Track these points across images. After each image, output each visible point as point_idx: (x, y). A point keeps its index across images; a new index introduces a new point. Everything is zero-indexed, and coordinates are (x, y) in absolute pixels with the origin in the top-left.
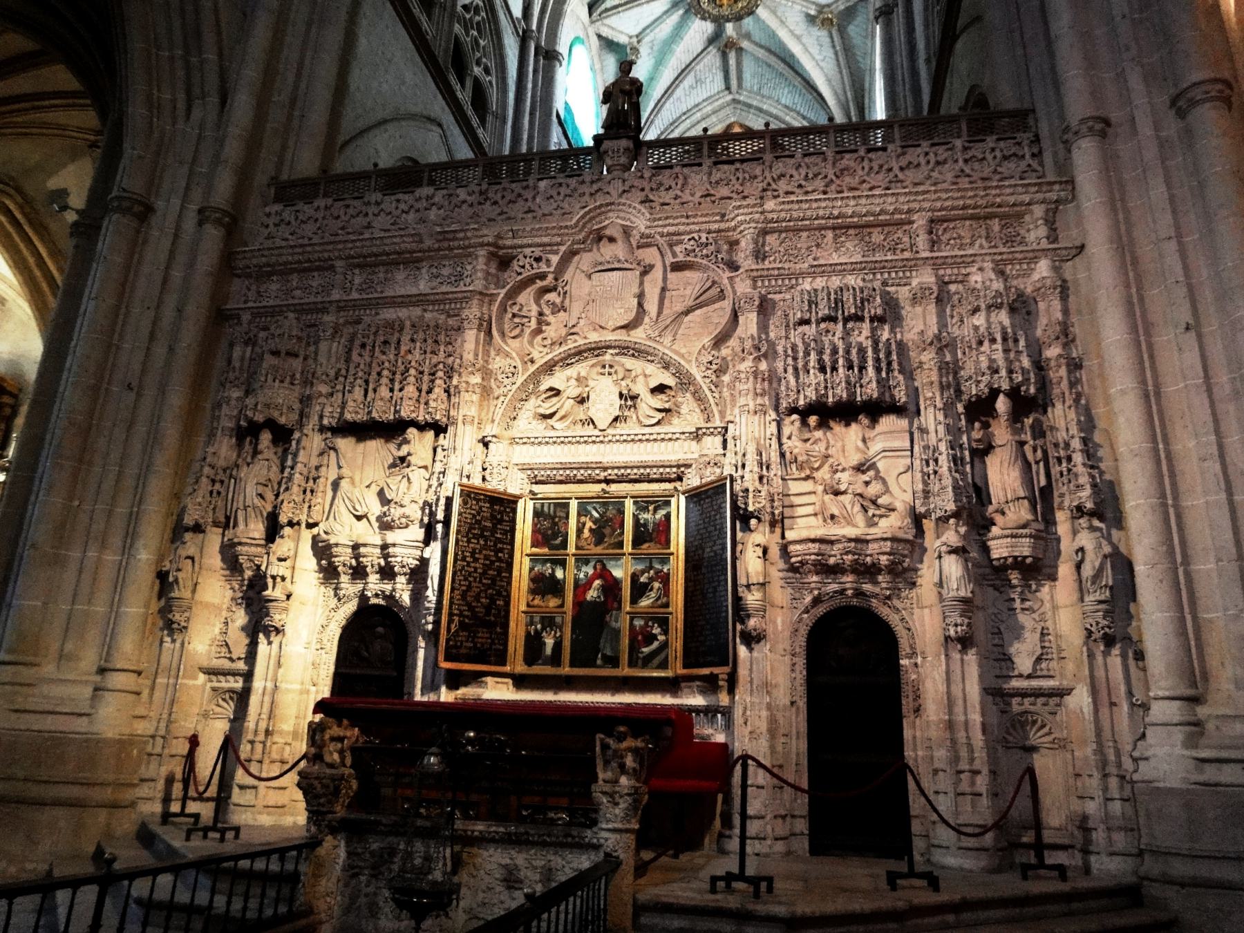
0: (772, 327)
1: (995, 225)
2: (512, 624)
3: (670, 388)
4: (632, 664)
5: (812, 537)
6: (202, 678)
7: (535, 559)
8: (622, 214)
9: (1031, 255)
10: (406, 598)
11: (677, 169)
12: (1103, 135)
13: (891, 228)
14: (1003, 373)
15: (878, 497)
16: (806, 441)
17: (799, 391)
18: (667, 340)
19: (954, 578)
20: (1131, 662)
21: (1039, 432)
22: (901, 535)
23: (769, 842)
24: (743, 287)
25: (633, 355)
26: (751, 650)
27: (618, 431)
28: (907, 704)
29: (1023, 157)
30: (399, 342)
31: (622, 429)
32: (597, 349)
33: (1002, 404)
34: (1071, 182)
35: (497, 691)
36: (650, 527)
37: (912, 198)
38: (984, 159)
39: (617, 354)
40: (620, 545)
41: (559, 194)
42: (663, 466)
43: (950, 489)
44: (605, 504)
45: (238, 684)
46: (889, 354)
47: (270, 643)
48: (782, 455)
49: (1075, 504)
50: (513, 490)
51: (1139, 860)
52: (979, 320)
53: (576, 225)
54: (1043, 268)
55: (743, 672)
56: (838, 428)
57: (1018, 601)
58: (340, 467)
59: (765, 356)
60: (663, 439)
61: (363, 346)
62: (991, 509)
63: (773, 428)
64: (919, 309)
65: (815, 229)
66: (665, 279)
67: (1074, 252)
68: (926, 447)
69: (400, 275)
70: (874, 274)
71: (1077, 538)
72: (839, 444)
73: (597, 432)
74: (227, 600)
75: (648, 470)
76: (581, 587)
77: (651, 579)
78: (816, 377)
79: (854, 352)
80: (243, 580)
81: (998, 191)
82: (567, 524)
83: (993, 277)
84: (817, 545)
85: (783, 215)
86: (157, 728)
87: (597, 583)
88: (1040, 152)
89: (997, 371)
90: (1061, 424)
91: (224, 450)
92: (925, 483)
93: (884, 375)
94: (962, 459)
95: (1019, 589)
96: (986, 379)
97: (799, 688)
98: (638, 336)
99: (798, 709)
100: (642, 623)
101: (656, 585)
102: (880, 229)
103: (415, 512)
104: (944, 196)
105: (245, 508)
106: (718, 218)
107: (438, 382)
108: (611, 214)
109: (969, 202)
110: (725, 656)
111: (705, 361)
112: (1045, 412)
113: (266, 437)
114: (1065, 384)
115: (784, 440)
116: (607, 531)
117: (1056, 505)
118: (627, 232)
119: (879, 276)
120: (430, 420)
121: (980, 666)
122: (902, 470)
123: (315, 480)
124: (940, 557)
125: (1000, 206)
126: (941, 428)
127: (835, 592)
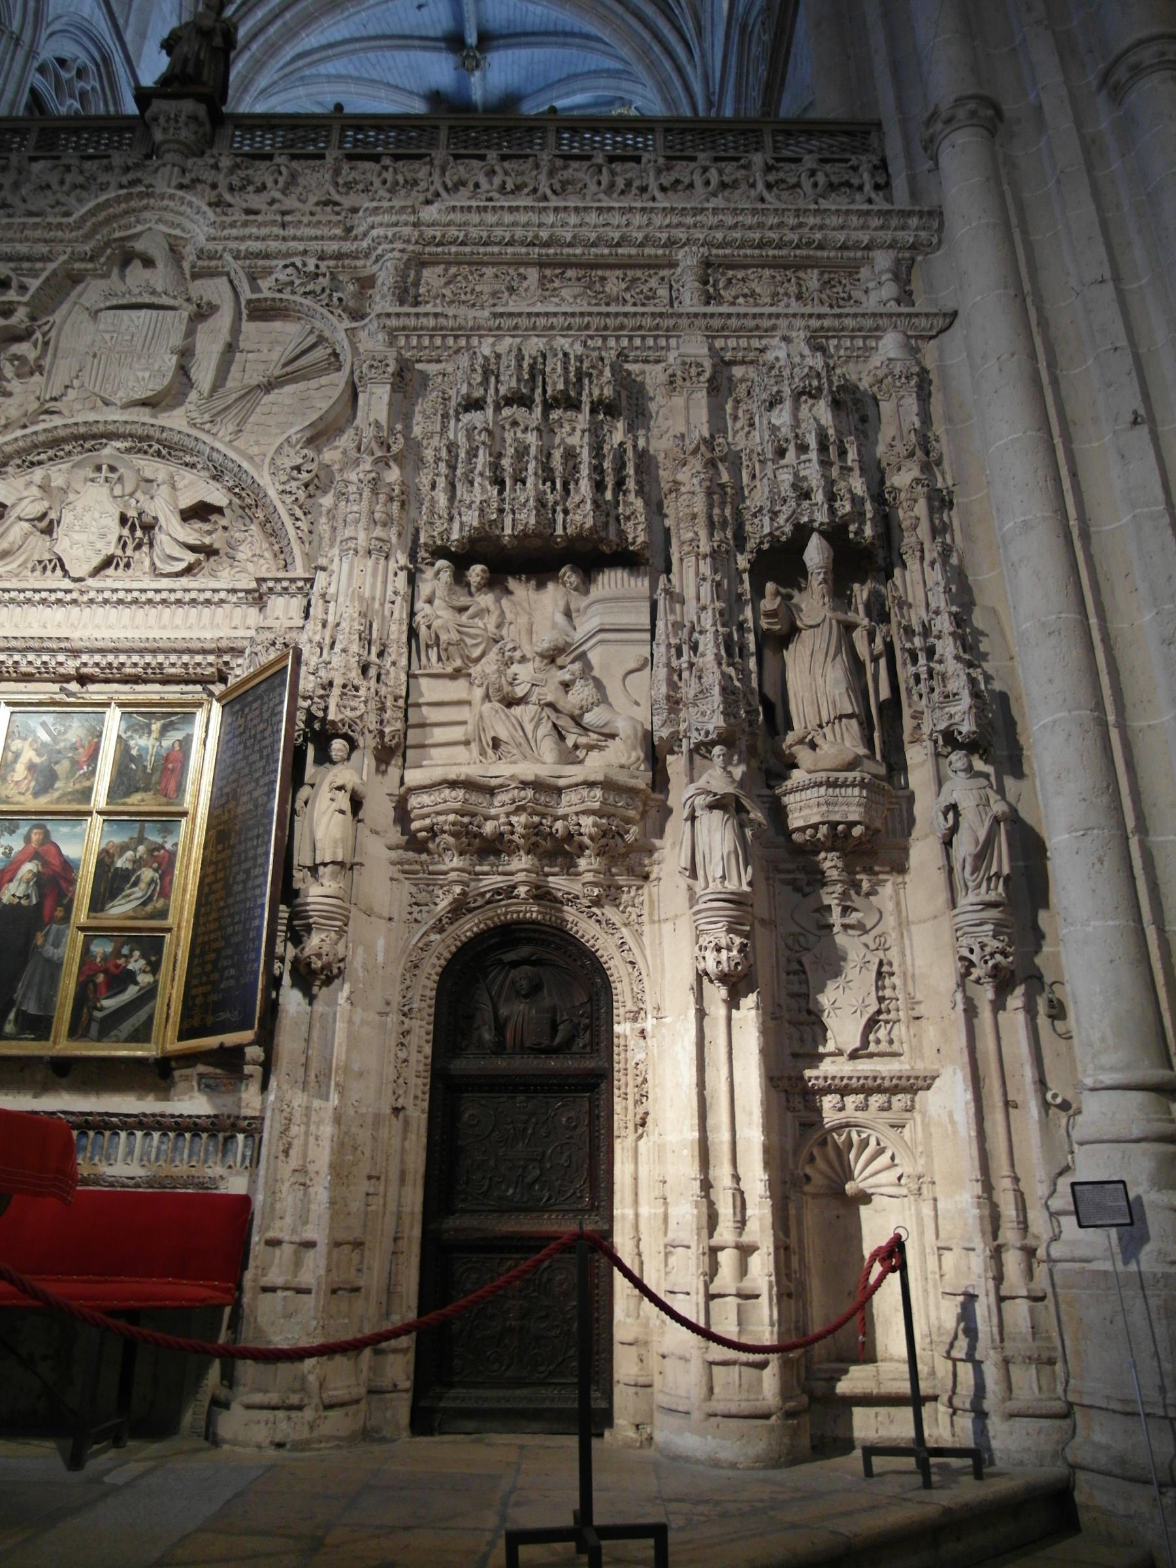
0: (418, 417)
1: (812, 279)
3: (219, 510)
4: (76, 1031)
5: (452, 776)
8: (169, 216)
9: (869, 323)
12: (992, 132)
13: (639, 273)
14: (819, 497)
15: (584, 710)
16: (462, 610)
17: (451, 519)
18: (226, 429)
19: (717, 857)
20: (1043, 1021)
21: (879, 612)
22: (622, 778)
23: (308, 1414)
24: (372, 341)
25: (159, 454)
26: (311, 998)
27: (110, 583)
28: (623, 1112)
29: (860, 188)
31: (113, 579)
33: (815, 553)
34: (936, 214)
37: (675, 220)
38: (798, 185)
39: (128, 450)
41: (62, 182)
42: (189, 651)
43: (716, 690)
46: (620, 466)
48: (413, 633)
49: (942, 726)
51: (1065, 1424)
52: (782, 417)
53: (79, 224)
54: (890, 345)
55: (288, 1042)
56: (521, 590)
57: (836, 911)
59: (399, 459)
60: (193, 601)
62: (790, 738)
63: (401, 582)
64: (678, 401)
65: (509, 264)
66: (236, 330)
67: (940, 323)
68: (678, 626)
70: (605, 338)
71: (945, 789)
72: (523, 620)
73: (67, 584)
75: (160, 658)
77: (138, 863)
78: (483, 490)
79: (557, 455)
81: (818, 221)
83: (807, 352)
84: (460, 793)
85: (453, 232)
87: (29, 867)
88: (888, 184)
89: (806, 495)
90: (915, 595)
92: (672, 686)
93: (609, 495)
94: (743, 648)
95: (839, 888)
96: (786, 511)
97: (413, 1081)
98: (175, 420)
99: (406, 1123)
100: (109, 948)
102: (619, 273)
104: (730, 220)
106: (338, 231)
108: (147, 215)
109: (774, 235)
111: (289, 463)
112: (889, 576)
114: (923, 531)
115: (420, 605)
117: (906, 737)
118: (175, 252)
119: (612, 343)
121: (764, 1031)
122: (633, 665)
124: (692, 818)
125: (821, 247)
126: (706, 589)
127: (498, 892)
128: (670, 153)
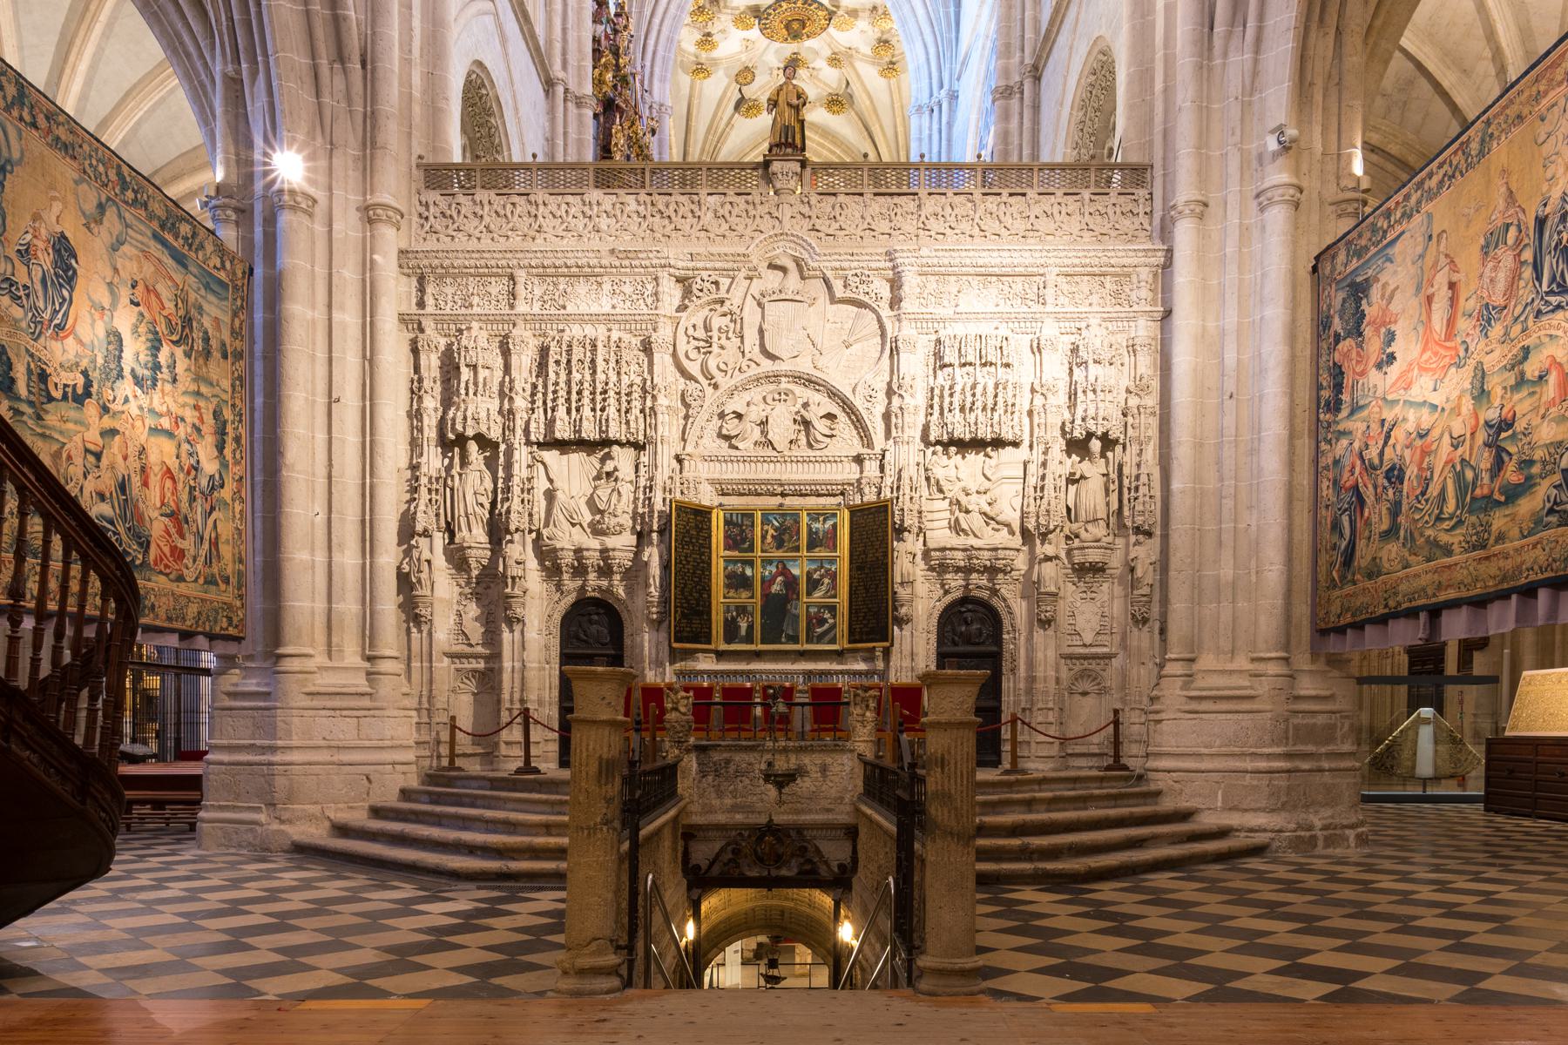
2: (714, 613)
4: (809, 640)
6: (446, 661)
7: (728, 561)
10: (621, 591)
11: (841, 198)
26: (901, 629)
30: (593, 361)
31: (796, 452)
32: (775, 377)
35: (706, 663)
36: (821, 535)
40: (797, 549)
44: (783, 515)
45: (481, 665)
47: (512, 631)
50: (706, 503)
58: (551, 481)
61: (557, 362)
69: (582, 288)
73: (775, 454)
74: (456, 597)
76: (767, 583)
77: (822, 576)
80: (470, 578)
82: (753, 531)
86: (420, 703)
91: (433, 461)
101: (826, 581)
103: (627, 521)
105: (467, 515)
107: (634, 403)
108: (781, 244)
110: (883, 634)
113: (473, 447)
116: (786, 537)
120: (632, 439)
123: (529, 490)
128: (1042, 190)
